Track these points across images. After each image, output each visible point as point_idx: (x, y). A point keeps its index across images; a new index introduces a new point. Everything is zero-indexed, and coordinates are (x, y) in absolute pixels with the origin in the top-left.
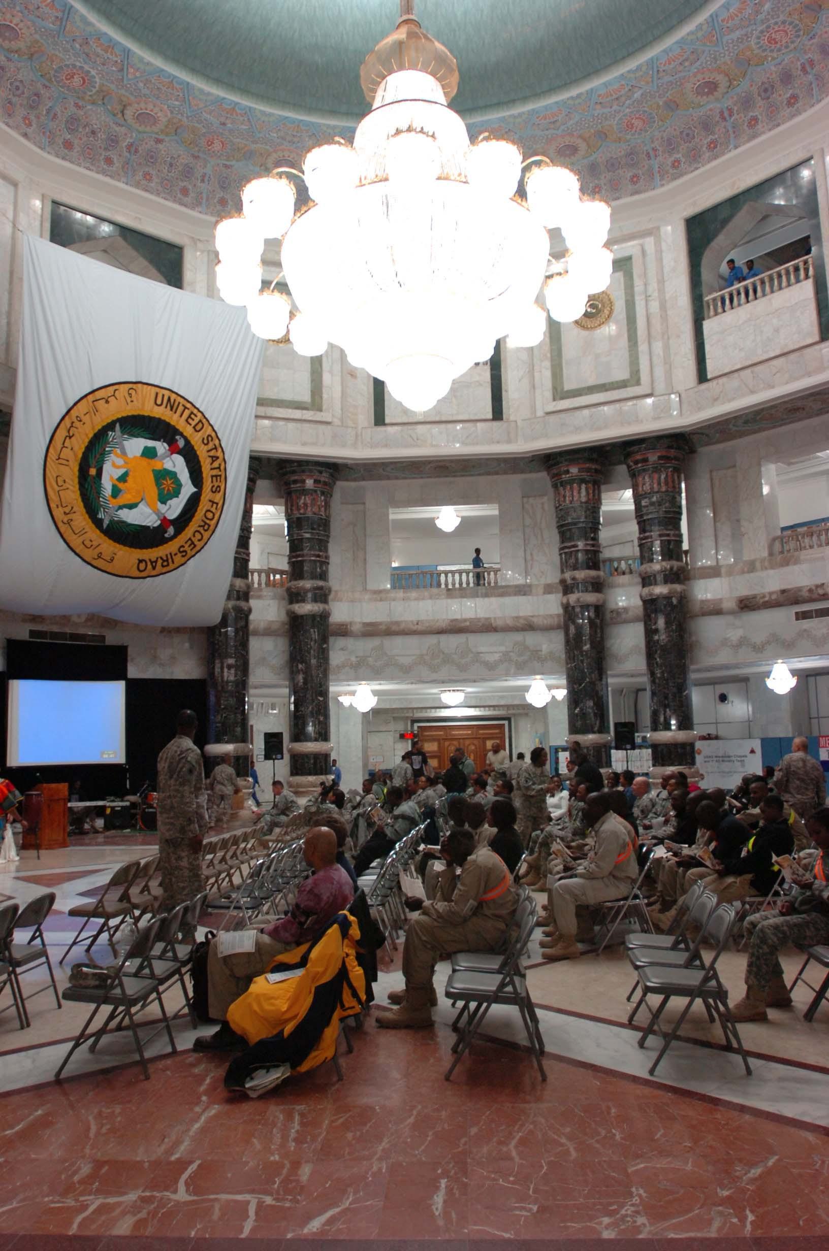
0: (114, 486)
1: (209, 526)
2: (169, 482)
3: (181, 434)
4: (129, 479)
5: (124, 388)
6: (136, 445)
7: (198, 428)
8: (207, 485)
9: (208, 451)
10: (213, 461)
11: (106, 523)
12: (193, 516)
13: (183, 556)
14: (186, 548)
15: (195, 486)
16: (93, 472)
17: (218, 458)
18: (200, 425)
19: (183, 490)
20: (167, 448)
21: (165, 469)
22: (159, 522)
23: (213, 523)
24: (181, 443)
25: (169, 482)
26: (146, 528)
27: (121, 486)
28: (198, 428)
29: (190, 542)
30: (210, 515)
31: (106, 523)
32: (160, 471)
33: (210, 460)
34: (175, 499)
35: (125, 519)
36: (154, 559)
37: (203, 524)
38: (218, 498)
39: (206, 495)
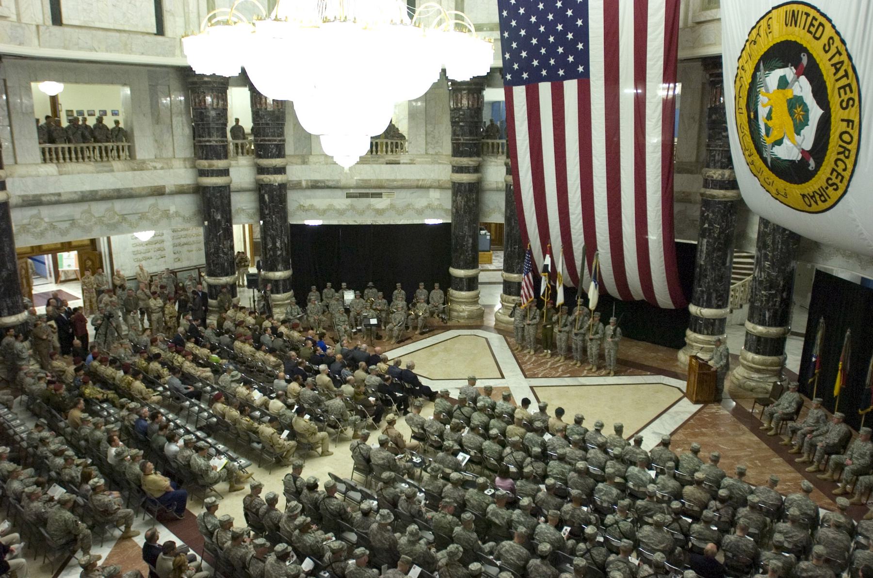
0: (766, 125)
1: (849, 151)
2: (799, 110)
3: (805, 50)
4: (773, 115)
5: (764, 23)
6: (773, 78)
7: (818, 35)
8: (834, 101)
9: (830, 60)
10: (837, 70)
11: (769, 160)
12: (827, 143)
13: (836, 190)
14: (834, 180)
15: (821, 107)
16: (752, 116)
17: (842, 62)
18: (821, 28)
19: (811, 116)
20: (795, 71)
21: (795, 96)
22: (800, 156)
23: (853, 147)
24: (805, 60)
25: (799, 110)
26: (793, 162)
27: (770, 123)
28: (818, 35)
29: (835, 174)
30: (846, 137)
31: (769, 160)
32: (791, 99)
33: (833, 70)
34: (806, 127)
35: (779, 156)
36: (812, 194)
37: (841, 150)
38: (851, 113)
39: (837, 114)
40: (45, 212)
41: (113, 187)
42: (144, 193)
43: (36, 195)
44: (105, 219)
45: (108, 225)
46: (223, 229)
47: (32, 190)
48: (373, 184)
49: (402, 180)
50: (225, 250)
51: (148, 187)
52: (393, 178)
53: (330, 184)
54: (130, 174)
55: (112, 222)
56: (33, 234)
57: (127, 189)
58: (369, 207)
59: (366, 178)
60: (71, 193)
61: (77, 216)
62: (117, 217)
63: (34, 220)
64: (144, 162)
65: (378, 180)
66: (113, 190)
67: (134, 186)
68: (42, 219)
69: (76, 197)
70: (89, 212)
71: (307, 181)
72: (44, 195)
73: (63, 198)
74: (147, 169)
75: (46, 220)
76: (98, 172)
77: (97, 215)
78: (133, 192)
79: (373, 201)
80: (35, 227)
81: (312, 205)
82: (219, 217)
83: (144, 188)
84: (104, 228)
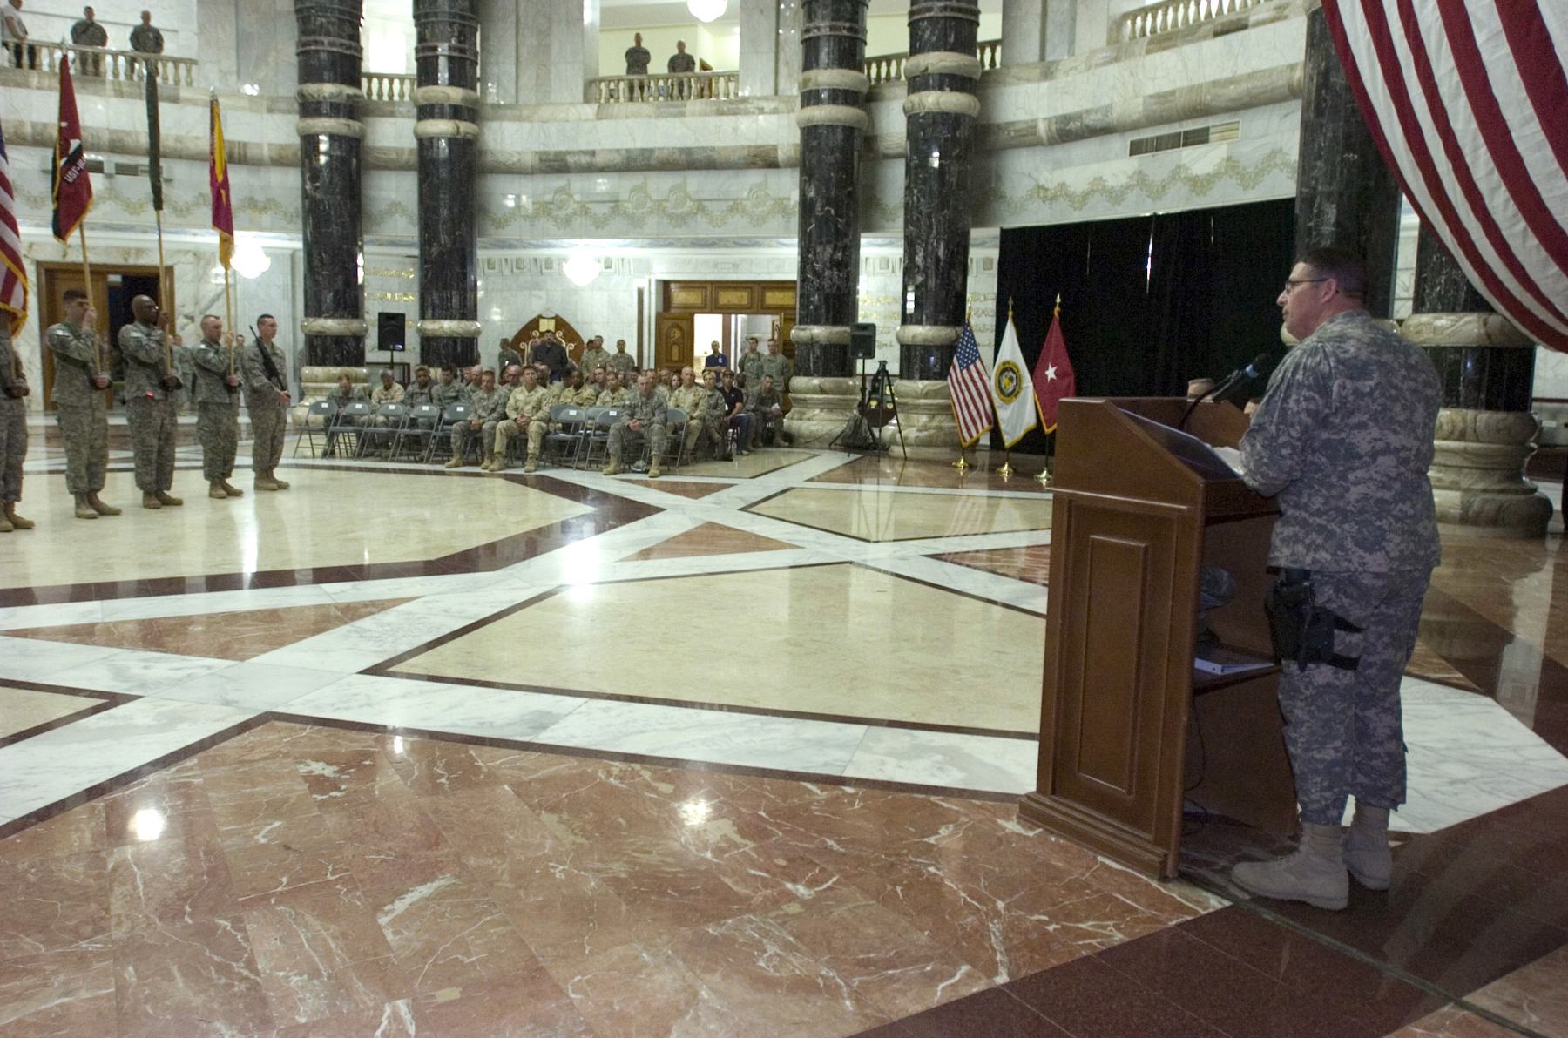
40: (577, 183)
41: (679, 145)
42: (734, 157)
43: (558, 154)
44: (668, 205)
45: (671, 217)
46: (818, 220)
47: (556, 142)
48: (1181, 102)
49: (1250, 76)
50: (818, 266)
51: (743, 147)
52: (1227, 74)
53: (1092, 120)
54: (713, 120)
55: (679, 211)
56: (555, 219)
57: (704, 149)
58: (1176, 173)
59: (1166, 87)
60: (610, 151)
61: (624, 196)
62: (689, 203)
63: (559, 197)
64: (745, 100)
65: (1191, 88)
66: (682, 150)
67: (718, 144)
68: (571, 196)
69: (618, 159)
70: (641, 189)
71: (1049, 120)
72: (569, 153)
73: (599, 160)
74: (747, 113)
75: (577, 197)
76: (658, 116)
77: (655, 197)
78: (715, 156)
79: (1187, 154)
80: (560, 208)
81: (1062, 185)
82: (812, 194)
83: (734, 149)
84: (666, 221)
